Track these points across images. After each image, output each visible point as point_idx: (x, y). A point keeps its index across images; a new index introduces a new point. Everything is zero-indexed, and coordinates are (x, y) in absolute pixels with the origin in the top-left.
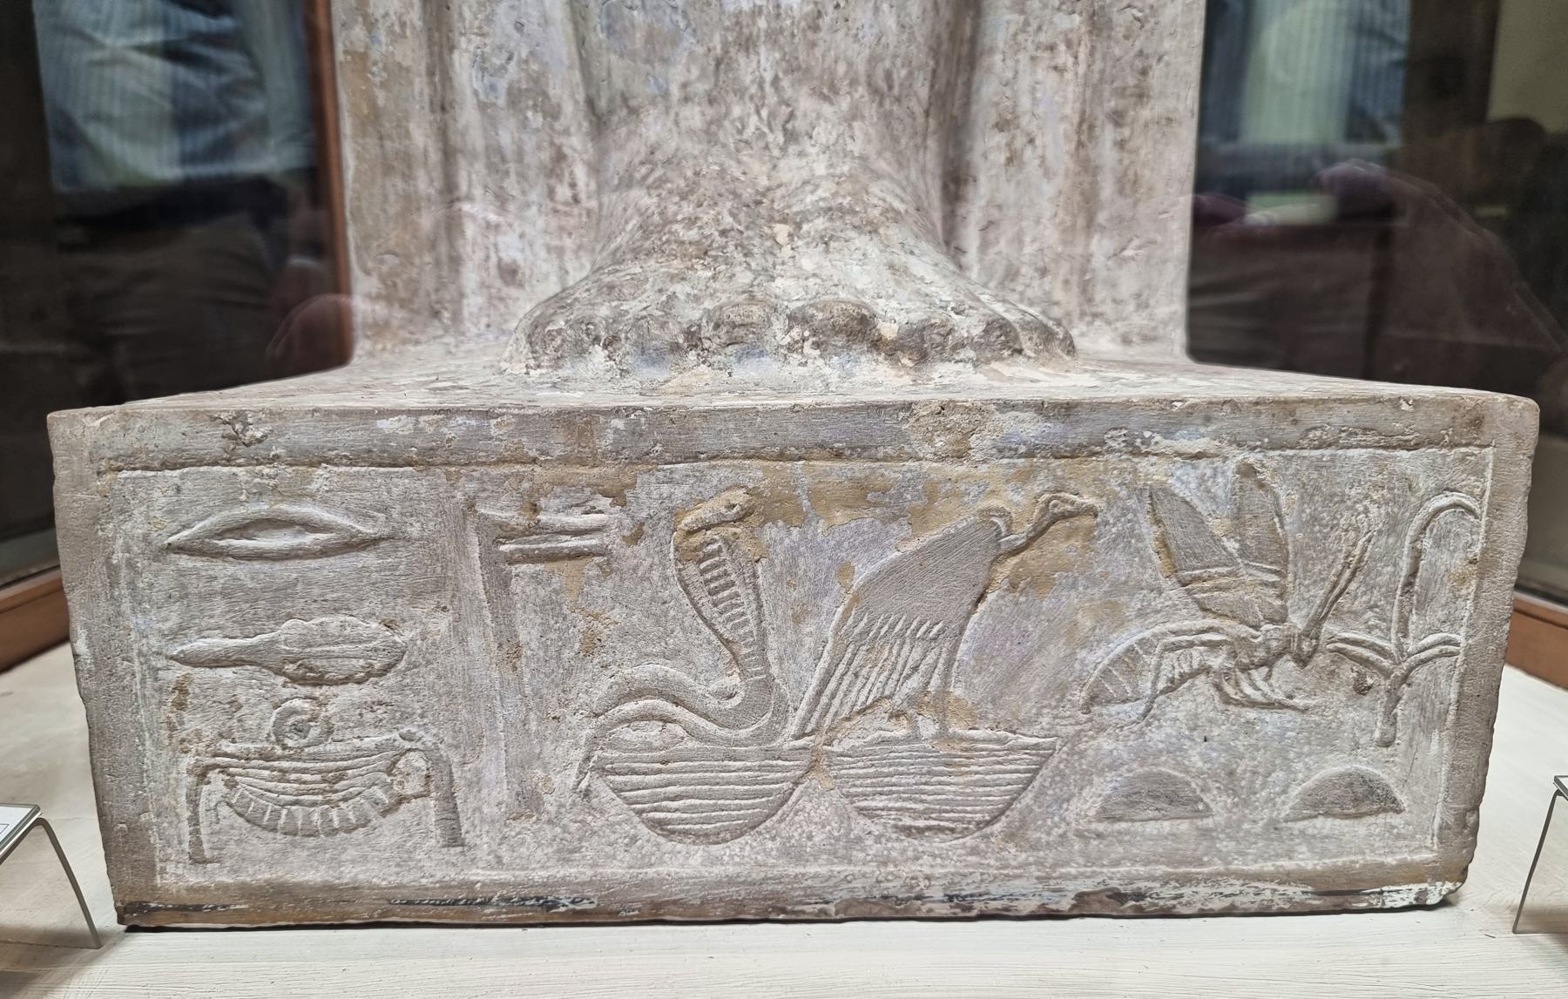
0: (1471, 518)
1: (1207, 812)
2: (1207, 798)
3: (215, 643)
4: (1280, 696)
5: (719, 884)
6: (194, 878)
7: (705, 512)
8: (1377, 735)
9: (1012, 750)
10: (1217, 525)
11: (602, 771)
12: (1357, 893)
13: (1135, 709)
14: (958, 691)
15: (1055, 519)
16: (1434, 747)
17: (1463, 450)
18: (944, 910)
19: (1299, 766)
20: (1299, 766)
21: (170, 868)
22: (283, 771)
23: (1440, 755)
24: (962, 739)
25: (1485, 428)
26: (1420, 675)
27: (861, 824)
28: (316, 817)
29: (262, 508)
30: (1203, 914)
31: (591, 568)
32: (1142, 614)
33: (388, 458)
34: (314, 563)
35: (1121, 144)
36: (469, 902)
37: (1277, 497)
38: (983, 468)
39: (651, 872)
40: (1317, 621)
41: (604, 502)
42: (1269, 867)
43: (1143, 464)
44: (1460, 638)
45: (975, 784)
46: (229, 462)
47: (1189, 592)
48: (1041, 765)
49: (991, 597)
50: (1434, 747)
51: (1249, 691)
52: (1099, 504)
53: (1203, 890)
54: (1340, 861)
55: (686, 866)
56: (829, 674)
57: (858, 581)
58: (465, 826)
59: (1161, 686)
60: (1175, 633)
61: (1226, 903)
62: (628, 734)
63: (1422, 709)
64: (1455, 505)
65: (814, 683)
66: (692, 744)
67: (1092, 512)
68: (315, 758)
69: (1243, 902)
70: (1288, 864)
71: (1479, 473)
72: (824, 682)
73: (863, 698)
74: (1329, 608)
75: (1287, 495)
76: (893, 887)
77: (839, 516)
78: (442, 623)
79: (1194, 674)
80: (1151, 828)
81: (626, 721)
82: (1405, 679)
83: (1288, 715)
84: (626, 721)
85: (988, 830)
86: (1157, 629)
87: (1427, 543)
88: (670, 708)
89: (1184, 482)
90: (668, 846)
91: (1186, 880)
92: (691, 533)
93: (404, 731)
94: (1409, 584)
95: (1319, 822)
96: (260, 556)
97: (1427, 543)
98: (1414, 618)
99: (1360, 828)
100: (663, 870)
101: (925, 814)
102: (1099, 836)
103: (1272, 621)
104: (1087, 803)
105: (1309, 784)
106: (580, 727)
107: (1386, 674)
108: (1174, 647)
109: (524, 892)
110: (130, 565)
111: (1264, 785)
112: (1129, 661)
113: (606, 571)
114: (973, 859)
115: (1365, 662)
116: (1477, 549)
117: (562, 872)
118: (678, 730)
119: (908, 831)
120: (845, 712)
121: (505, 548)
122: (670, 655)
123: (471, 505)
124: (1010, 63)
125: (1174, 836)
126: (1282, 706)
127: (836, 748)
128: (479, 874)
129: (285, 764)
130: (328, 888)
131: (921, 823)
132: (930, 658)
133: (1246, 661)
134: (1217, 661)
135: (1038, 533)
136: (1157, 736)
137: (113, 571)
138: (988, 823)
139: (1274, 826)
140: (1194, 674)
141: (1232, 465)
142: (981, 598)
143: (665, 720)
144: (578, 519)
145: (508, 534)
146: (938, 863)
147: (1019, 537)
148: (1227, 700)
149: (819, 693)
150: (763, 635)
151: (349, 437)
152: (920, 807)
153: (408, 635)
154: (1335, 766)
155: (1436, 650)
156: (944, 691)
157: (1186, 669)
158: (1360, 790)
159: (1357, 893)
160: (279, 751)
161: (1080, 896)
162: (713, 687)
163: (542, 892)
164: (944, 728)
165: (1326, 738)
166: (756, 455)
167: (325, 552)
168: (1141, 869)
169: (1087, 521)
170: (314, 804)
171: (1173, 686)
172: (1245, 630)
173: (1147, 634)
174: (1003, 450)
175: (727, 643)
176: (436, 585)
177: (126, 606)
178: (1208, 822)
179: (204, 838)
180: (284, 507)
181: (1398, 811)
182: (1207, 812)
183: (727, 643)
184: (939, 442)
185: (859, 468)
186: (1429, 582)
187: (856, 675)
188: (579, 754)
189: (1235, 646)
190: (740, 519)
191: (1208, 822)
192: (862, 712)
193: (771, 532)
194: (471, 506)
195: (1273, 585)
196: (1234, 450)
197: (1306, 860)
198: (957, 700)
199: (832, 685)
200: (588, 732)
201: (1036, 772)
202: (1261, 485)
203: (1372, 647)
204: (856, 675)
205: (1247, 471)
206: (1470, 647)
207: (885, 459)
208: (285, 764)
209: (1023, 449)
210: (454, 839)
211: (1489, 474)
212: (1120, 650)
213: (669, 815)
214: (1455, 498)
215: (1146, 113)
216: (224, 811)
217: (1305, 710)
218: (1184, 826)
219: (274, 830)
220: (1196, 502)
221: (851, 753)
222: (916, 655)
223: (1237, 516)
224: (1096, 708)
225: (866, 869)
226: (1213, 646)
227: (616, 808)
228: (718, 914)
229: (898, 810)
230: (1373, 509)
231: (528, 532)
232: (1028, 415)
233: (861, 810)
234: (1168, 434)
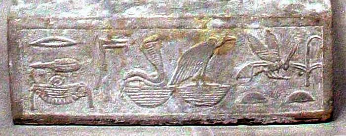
0: (320, 40)
2: (267, 98)
3: (40, 63)
5: (153, 117)
6: (31, 114)
7: (149, 39)
8: (305, 84)
17: (316, 27)
22: (53, 90)
23: (321, 87)
24: (208, 86)
25: (320, 22)
27: (186, 104)
28: (60, 101)
29: (51, 37)
31: (123, 49)
33: (78, 28)
36: (95, 120)
40: (288, 61)
43: (245, 30)
44: (321, 63)
46: (46, 28)
47: (258, 56)
48: (227, 92)
49: (214, 56)
59: (254, 74)
60: (256, 63)
62: (131, 84)
64: (316, 37)
66: (146, 86)
69: (279, 121)
72: (177, 73)
73: (185, 76)
75: (277, 36)
78: (89, 60)
81: (132, 81)
82: (310, 72)
84: (132, 81)
85: (215, 106)
88: (142, 79)
89: (255, 34)
91: (264, 116)
95: (294, 103)
96: (51, 46)
97: (310, 45)
98: (311, 60)
99: (305, 104)
101: (201, 102)
103: (277, 61)
105: (290, 95)
106: (121, 82)
108: (256, 67)
109: (108, 118)
113: (127, 50)
116: (322, 46)
117: (116, 114)
120: (182, 80)
122: (142, 67)
123: (97, 36)
125: (259, 107)
126: (282, 79)
127: (179, 88)
128: (97, 114)
131: (200, 104)
134: (266, 69)
135: (223, 43)
136: (255, 85)
138: (215, 104)
139: (283, 105)
140: (261, 72)
141: (264, 31)
143: (140, 81)
144: (120, 40)
146: (204, 113)
147: (219, 43)
151: (70, 25)
152: (200, 100)
155: (316, 67)
156: (204, 75)
157: (259, 71)
163: (112, 118)
165: (293, 85)
167: (65, 46)
169: (234, 41)
171: (256, 75)
172: (271, 63)
173: (249, 64)
174: (214, 27)
176: (89, 53)
181: (312, 100)
183: (154, 65)
186: (312, 52)
187: (184, 72)
189: (269, 66)
192: (185, 80)
195: (276, 54)
197: (291, 112)
198: (207, 77)
200: (122, 84)
202: (272, 34)
204: (184, 72)
207: (188, 28)
209: (218, 27)
210: (91, 106)
211: (322, 31)
216: (39, 99)
217: (287, 79)
219: (50, 103)
223: (267, 40)
224: (239, 79)
226: (265, 66)
227: (128, 99)
229: (195, 101)
231: (110, 43)
234: (249, 24)
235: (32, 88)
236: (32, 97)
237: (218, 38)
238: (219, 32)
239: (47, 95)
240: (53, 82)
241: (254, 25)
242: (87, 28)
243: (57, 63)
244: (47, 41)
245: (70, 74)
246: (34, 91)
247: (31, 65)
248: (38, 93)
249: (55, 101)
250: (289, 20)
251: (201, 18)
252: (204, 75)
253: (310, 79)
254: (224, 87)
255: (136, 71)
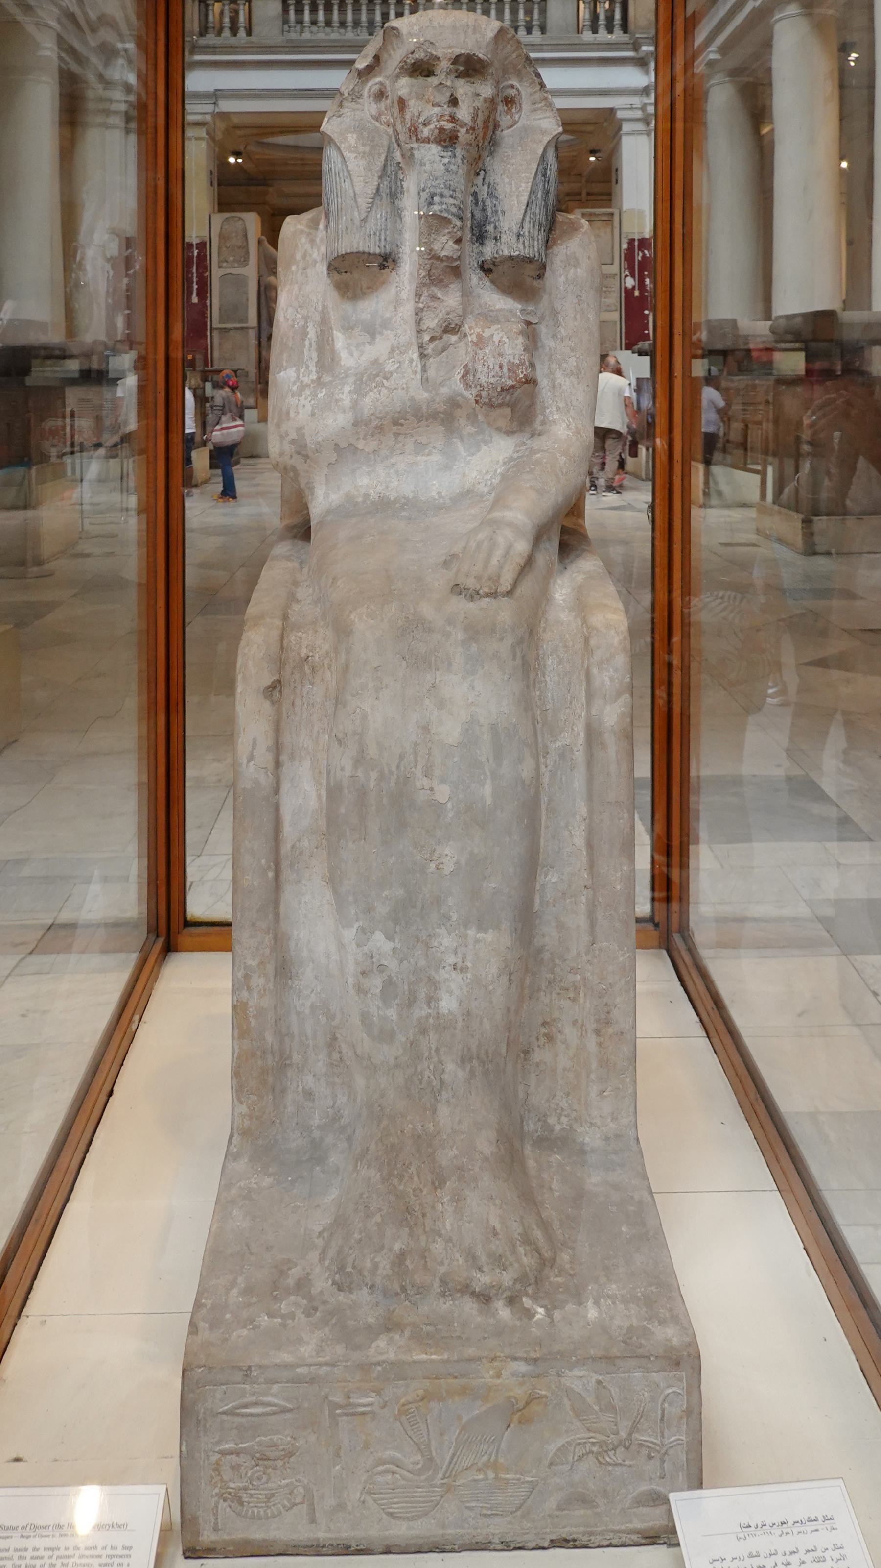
1: (597, 1506)
4: (620, 1461)
6: (214, 1537)
7: (409, 1398)
9: (523, 1483)
10: (590, 1400)
11: (370, 1493)
12: (659, 1537)
13: (566, 1467)
14: (501, 1460)
15: (533, 1399)
16: (681, 1478)
18: (499, 1547)
19: (630, 1487)
20: (630, 1487)
21: (205, 1532)
26: (671, 1452)
28: (262, 1513)
30: (599, 1547)
31: (368, 1418)
32: (567, 1432)
33: (297, 1381)
34: (270, 1417)
35: (600, 1044)
36: (318, 1546)
37: (610, 1391)
38: (507, 1381)
39: (387, 1533)
40: (630, 1434)
41: (374, 1394)
42: (623, 1527)
44: (683, 1438)
45: (511, 1496)
49: (512, 1426)
50: (681, 1478)
51: (608, 1459)
52: (549, 1394)
53: (599, 1537)
54: (651, 1524)
55: (400, 1531)
56: (454, 1455)
57: (464, 1421)
58: (317, 1515)
59: (576, 1458)
61: (607, 1543)
62: (380, 1479)
63: (674, 1463)
65: (448, 1458)
66: (403, 1482)
67: (546, 1397)
68: (263, 1489)
69: (614, 1542)
70: (630, 1526)
71: (681, 1380)
72: (452, 1458)
74: (634, 1428)
76: (479, 1539)
77: (457, 1398)
78: (313, 1438)
79: (588, 1454)
80: (577, 1513)
81: (380, 1474)
82: (666, 1453)
83: (624, 1468)
84: (380, 1474)
85: (515, 1514)
86: (572, 1437)
87: (666, 1405)
88: (395, 1468)
90: (393, 1522)
91: (591, 1534)
92: (403, 1405)
93: (297, 1477)
94: (662, 1419)
95: (641, 1508)
96: (251, 1415)
98: (666, 1430)
100: (391, 1532)
101: (490, 1509)
102: (557, 1516)
104: (552, 1503)
105: (634, 1494)
107: (659, 1452)
108: (579, 1444)
109: (339, 1542)
110: (205, 1419)
111: (618, 1495)
112: (562, 1450)
114: (510, 1526)
115: (649, 1447)
118: (398, 1476)
119: (485, 1515)
120: (460, 1469)
121: (338, 1411)
124: (548, 995)
126: (621, 1464)
127: (457, 1484)
129: (253, 1492)
130: (265, 1540)
131: (489, 1512)
132: (490, 1450)
133: (605, 1449)
134: (595, 1449)
135: (527, 1404)
137: (198, 1422)
140: (588, 1454)
141: (594, 1380)
142: (509, 1426)
143: (393, 1473)
145: (338, 1406)
146: (497, 1528)
147: (521, 1405)
148: (600, 1463)
149: (450, 1463)
150: (429, 1440)
153: (301, 1442)
154: (644, 1487)
156: (496, 1461)
158: (655, 1496)
159: (659, 1537)
160: (251, 1486)
161: (552, 1541)
162: (411, 1460)
163: (345, 1542)
164: (497, 1475)
166: (428, 1378)
167: (274, 1413)
168: (574, 1529)
170: (262, 1507)
171: (580, 1458)
172: (604, 1438)
173: (569, 1439)
174: (513, 1375)
175: (416, 1444)
177: (201, 1434)
178: (598, 1510)
179: (219, 1520)
180: (261, 1398)
182: (597, 1506)
183: (416, 1444)
184: (491, 1373)
185: (463, 1381)
188: (360, 1487)
189: (601, 1444)
190: (422, 1399)
191: (598, 1510)
193: (433, 1404)
194: (327, 1398)
196: (593, 1375)
197: (638, 1525)
199: (455, 1460)
200: (363, 1478)
201: (532, 1492)
202: (604, 1387)
203: (652, 1442)
205: (599, 1382)
206: (687, 1442)
208: (253, 1492)
210: (313, 1521)
212: (559, 1445)
213: (396, 1510)
214: (674, 1389)
215: (610, 1031)
216: (228, 1509)
217: (630, 1466)
218: (589, 1512)
220: (582, 1392)
221: (463, 1485)
222: (485, 1448)
223: (597, 1398)
225: (469, 1531)
226: (593, 1443)
228: (413, 1550)
230: (646, 1393)
232: (522, 1363)
233: (467, 1508)
235: (217, 1490)
236: (217, 1507)
237: (520, 1393)
238: (521, 1384)
239: (241, 1503)
240: (251, 1480)
241: (577, 1372)
242: (313, 1380)
243: (260, 1444)
244: (246, 1406)
245: (279, 1463)
246: (220, 1496)
247: (218, 1449)
248: (225, 1500)
249: (253, 1512)
250: (632, 1363)
251: (494, 1359)
252: (496, 1461)
253: (665, 1465)
254: (527, 1482)
255: (389, 1453)
